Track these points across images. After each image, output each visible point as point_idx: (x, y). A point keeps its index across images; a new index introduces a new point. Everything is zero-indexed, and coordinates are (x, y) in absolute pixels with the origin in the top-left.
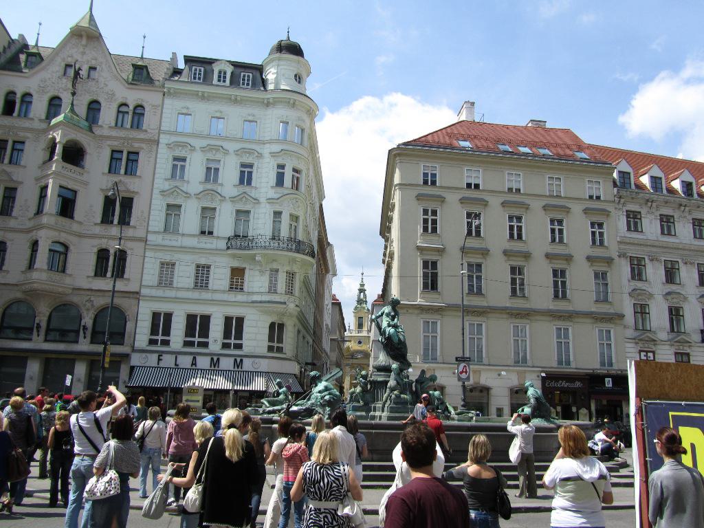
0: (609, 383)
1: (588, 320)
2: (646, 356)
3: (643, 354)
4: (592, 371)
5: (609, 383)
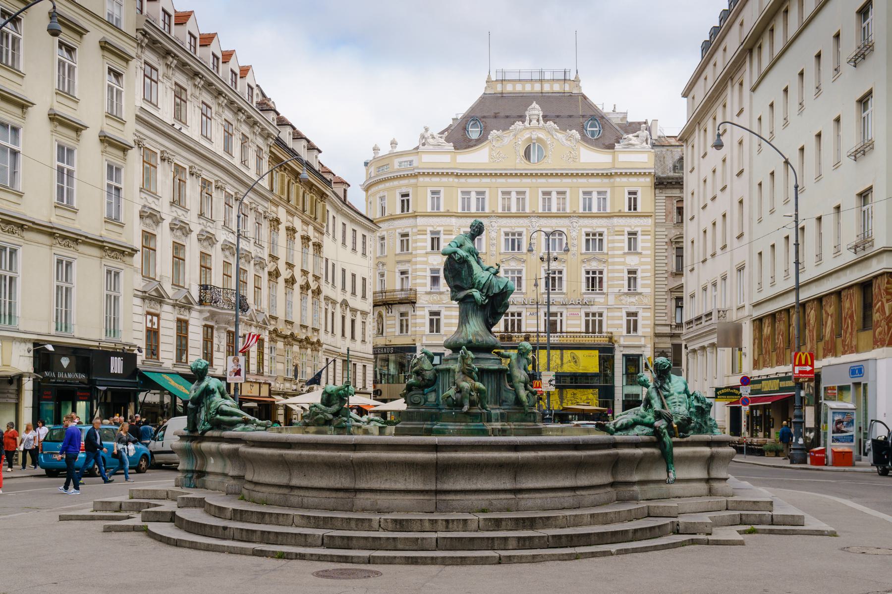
0: (117, 365)
1: (96, 252)
2: (151, 321)
3: (149, 317)
4: (97, 344)
5: (117, 365)
